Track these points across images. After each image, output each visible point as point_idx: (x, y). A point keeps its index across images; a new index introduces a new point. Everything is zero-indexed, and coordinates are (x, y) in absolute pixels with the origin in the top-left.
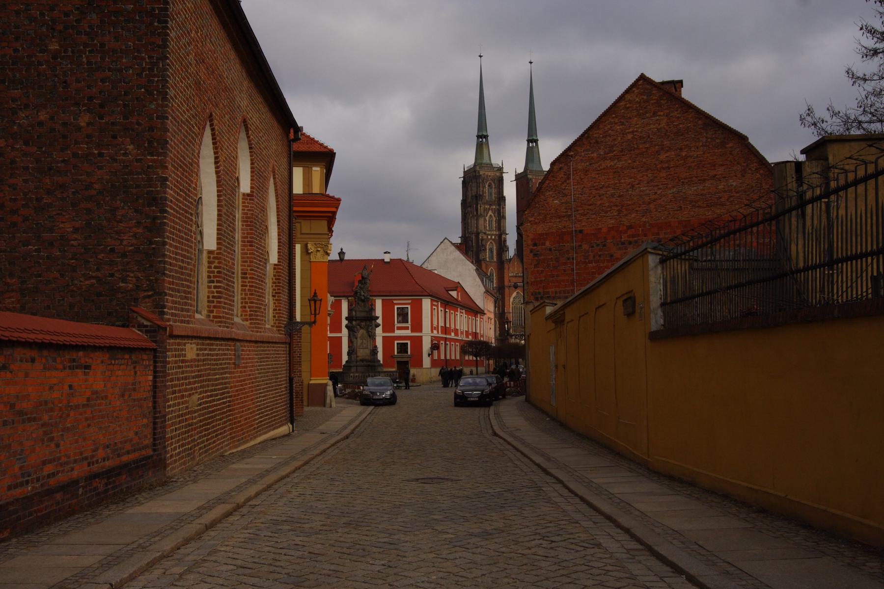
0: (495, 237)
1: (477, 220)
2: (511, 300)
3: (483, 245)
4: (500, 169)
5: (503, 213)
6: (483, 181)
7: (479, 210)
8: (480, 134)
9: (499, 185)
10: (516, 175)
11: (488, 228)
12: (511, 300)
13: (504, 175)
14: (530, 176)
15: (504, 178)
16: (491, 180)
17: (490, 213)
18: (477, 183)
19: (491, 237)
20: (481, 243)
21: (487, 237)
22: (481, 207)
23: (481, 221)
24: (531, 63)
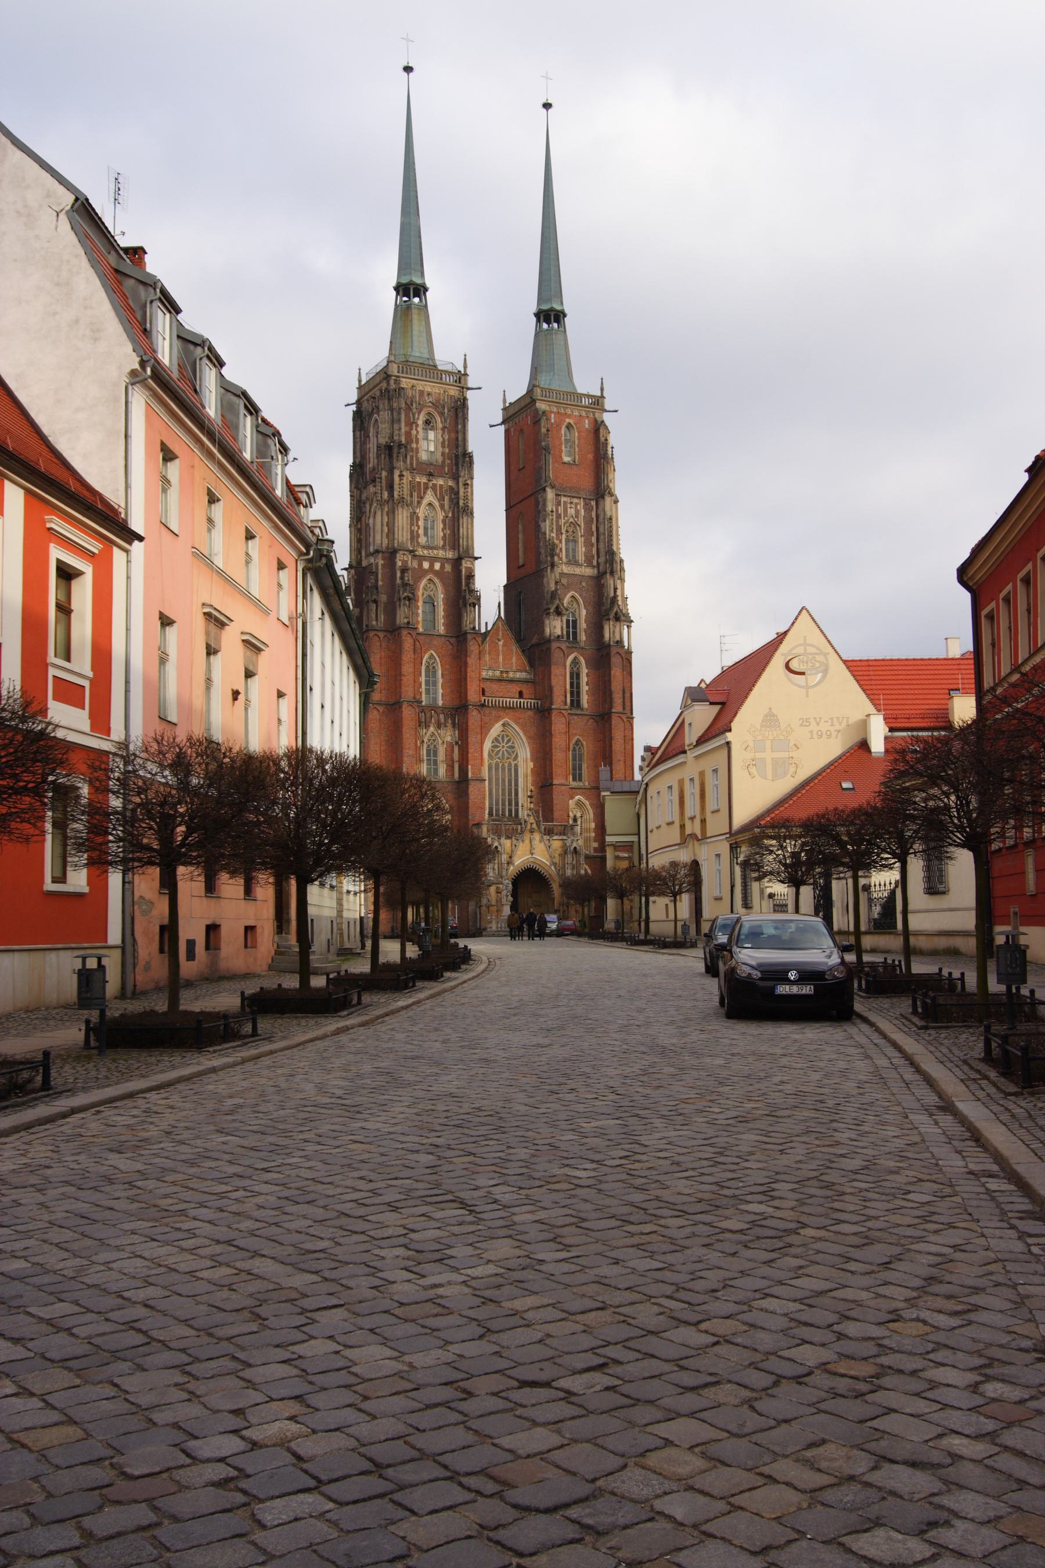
0: (442, 567)
1: (392, 513)
3: (405, 585)
4: (460, 378)
5: (466, 498)
6: (409, 408)
7: (396, 487)
8: (405, 280)
9: (457, 424)
10: (504, 409)
11: (422, 540)
12: (487, 745)
13: (469, 394)
14: (541, 406)
15: (471, 404)
16: (435, 405)
17: (429, 497)
18: (392, 409)
19: (432, 566)
20: (402, 578)
21: (420, 565)
22: (401, 476)
23: (402, 517)
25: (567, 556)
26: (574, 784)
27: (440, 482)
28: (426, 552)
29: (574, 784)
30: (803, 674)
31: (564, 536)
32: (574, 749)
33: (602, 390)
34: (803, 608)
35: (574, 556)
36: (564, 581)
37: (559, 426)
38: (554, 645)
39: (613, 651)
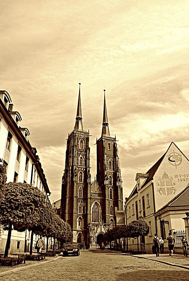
0: (83, 169)
2: (92, 207)
5: (88, 156)
7: (74, 153)
10: (97, 141)
11: (79, 164)
12: (92, 207)
13: (89, 137)
14: (103, 140)
15: (89, 138)
17: (81, 156)
19: (81, 169)
20: (75, 171)
21: (79, 169)
22: (75, 151)
24: (105, 90)
25: (109, 168)
26: (111, 215)
27: (83, 153)
28: (80, 167)
29: (111, 215)
30: (174, 161)
31: (108, 164)
32: (111, 208)
33: (115, 137)
34: (172, 142)
35: (111, 169)
36: (108, 173)
37: (107, 143)
38: (106, 186)
39: (119, 187)
